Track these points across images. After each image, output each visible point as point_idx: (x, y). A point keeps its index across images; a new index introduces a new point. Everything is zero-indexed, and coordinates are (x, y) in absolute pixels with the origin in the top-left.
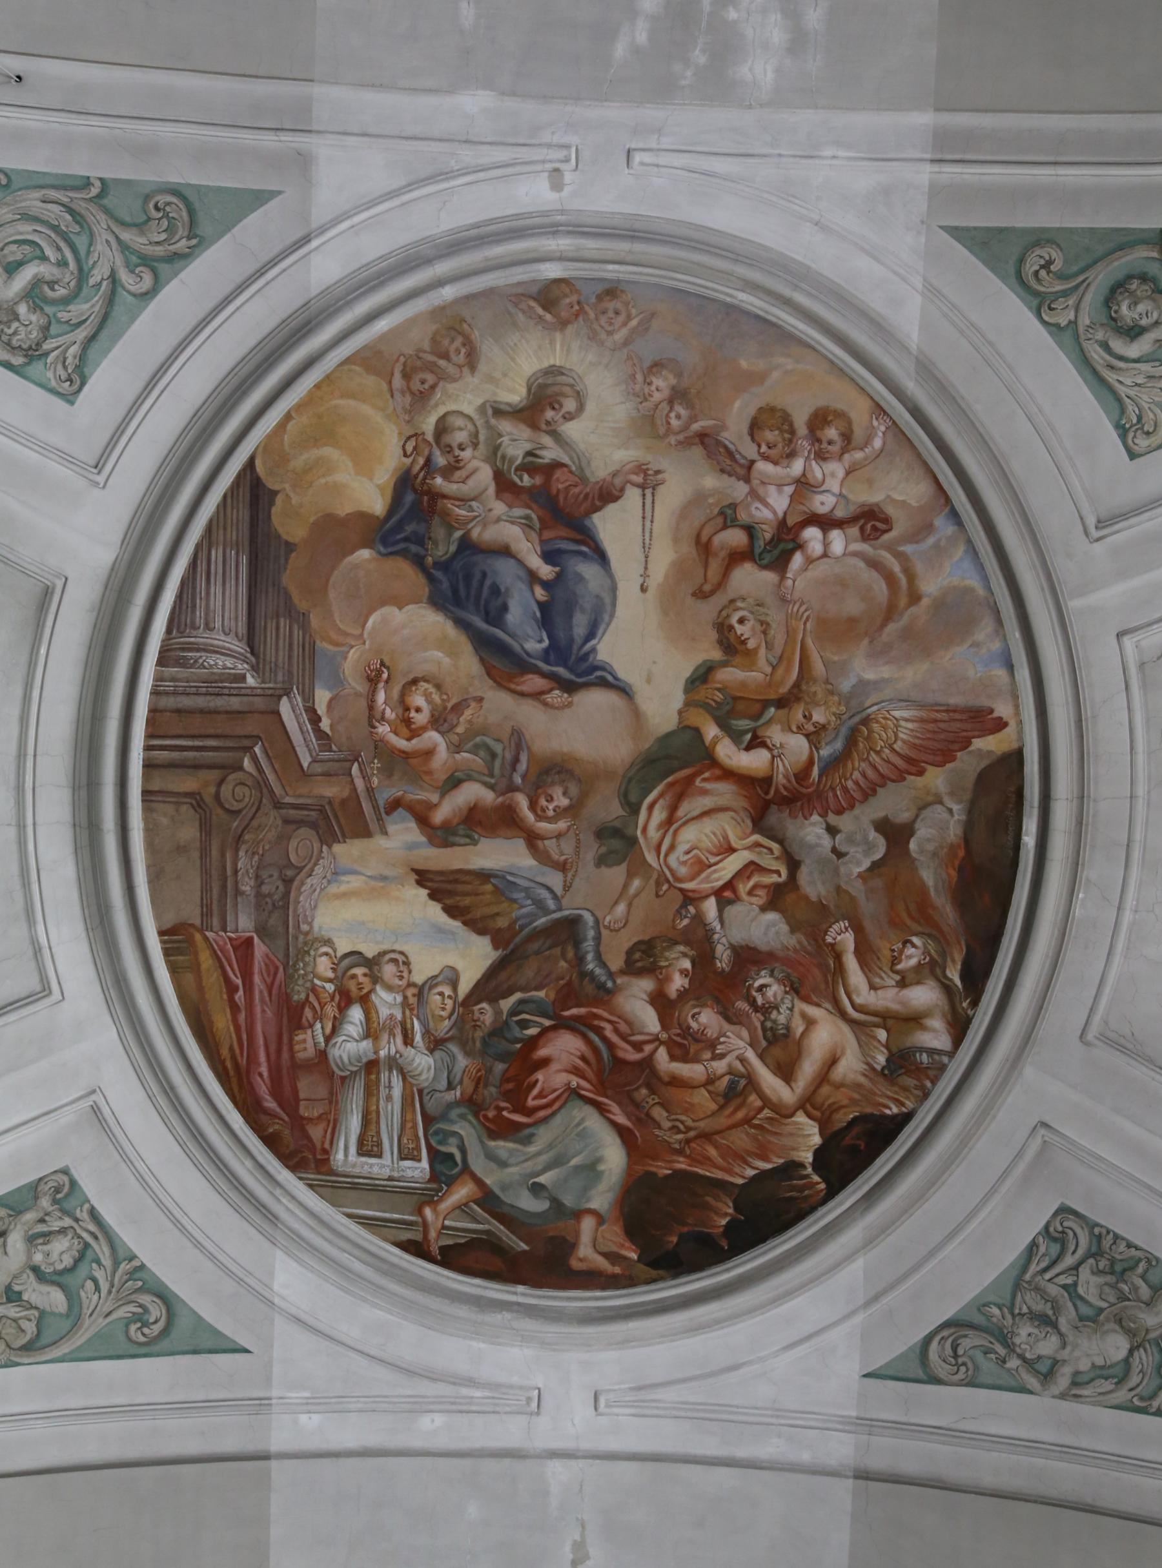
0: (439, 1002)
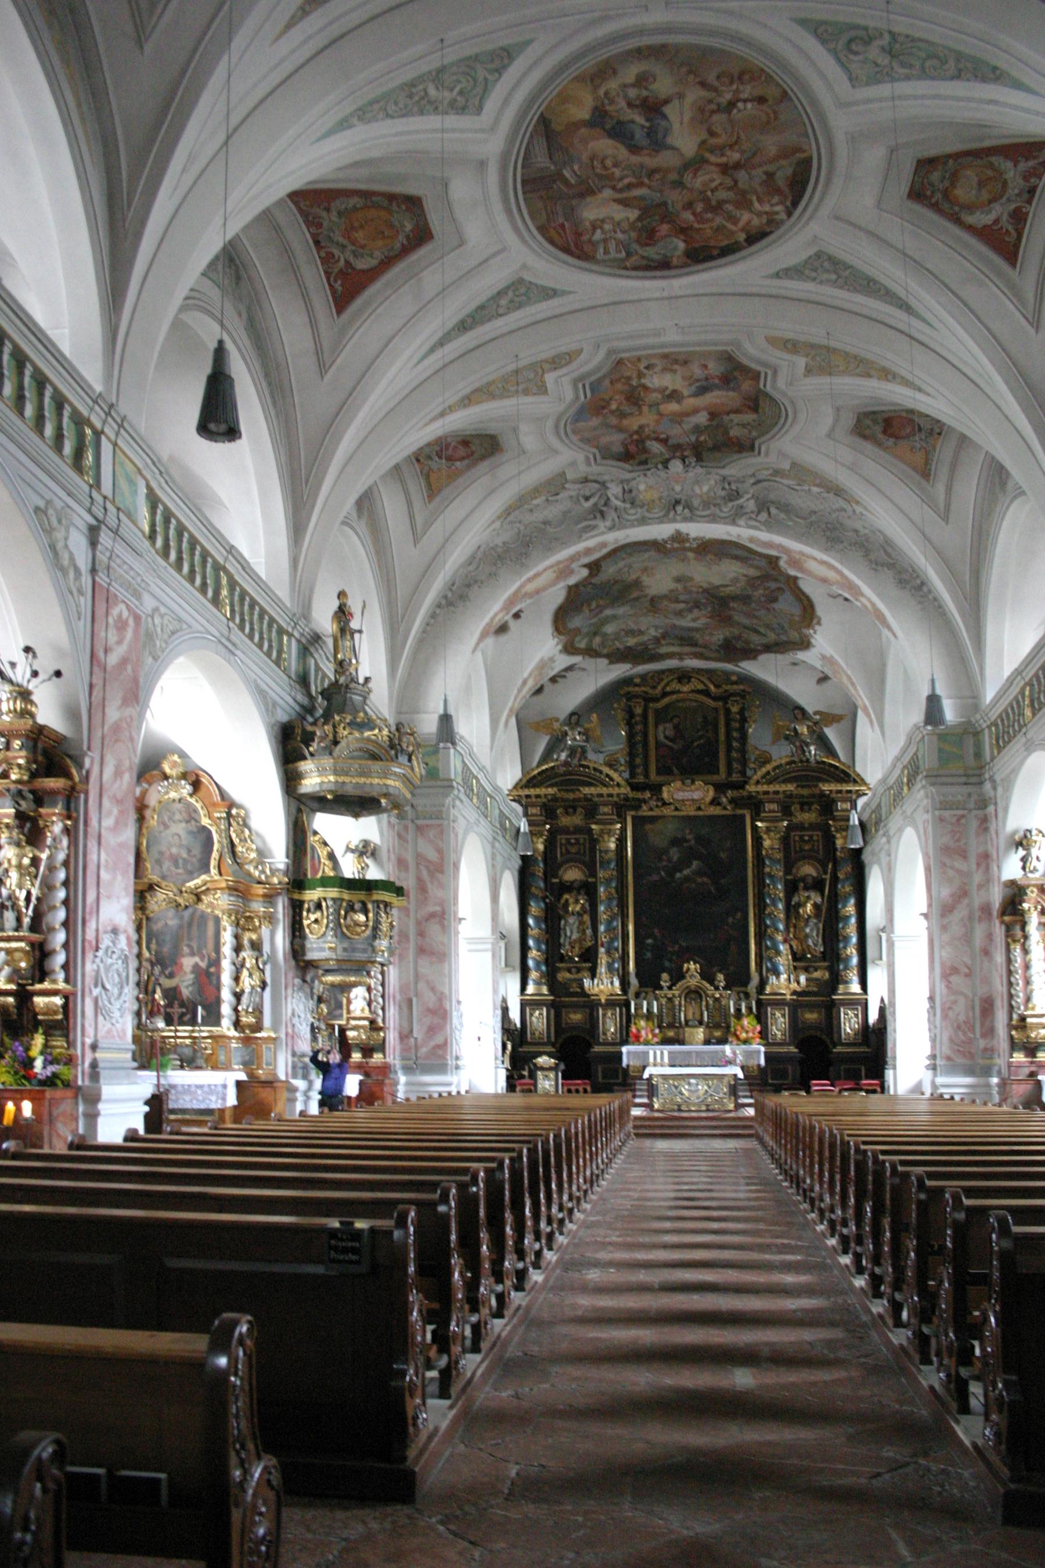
0: (625, 225)
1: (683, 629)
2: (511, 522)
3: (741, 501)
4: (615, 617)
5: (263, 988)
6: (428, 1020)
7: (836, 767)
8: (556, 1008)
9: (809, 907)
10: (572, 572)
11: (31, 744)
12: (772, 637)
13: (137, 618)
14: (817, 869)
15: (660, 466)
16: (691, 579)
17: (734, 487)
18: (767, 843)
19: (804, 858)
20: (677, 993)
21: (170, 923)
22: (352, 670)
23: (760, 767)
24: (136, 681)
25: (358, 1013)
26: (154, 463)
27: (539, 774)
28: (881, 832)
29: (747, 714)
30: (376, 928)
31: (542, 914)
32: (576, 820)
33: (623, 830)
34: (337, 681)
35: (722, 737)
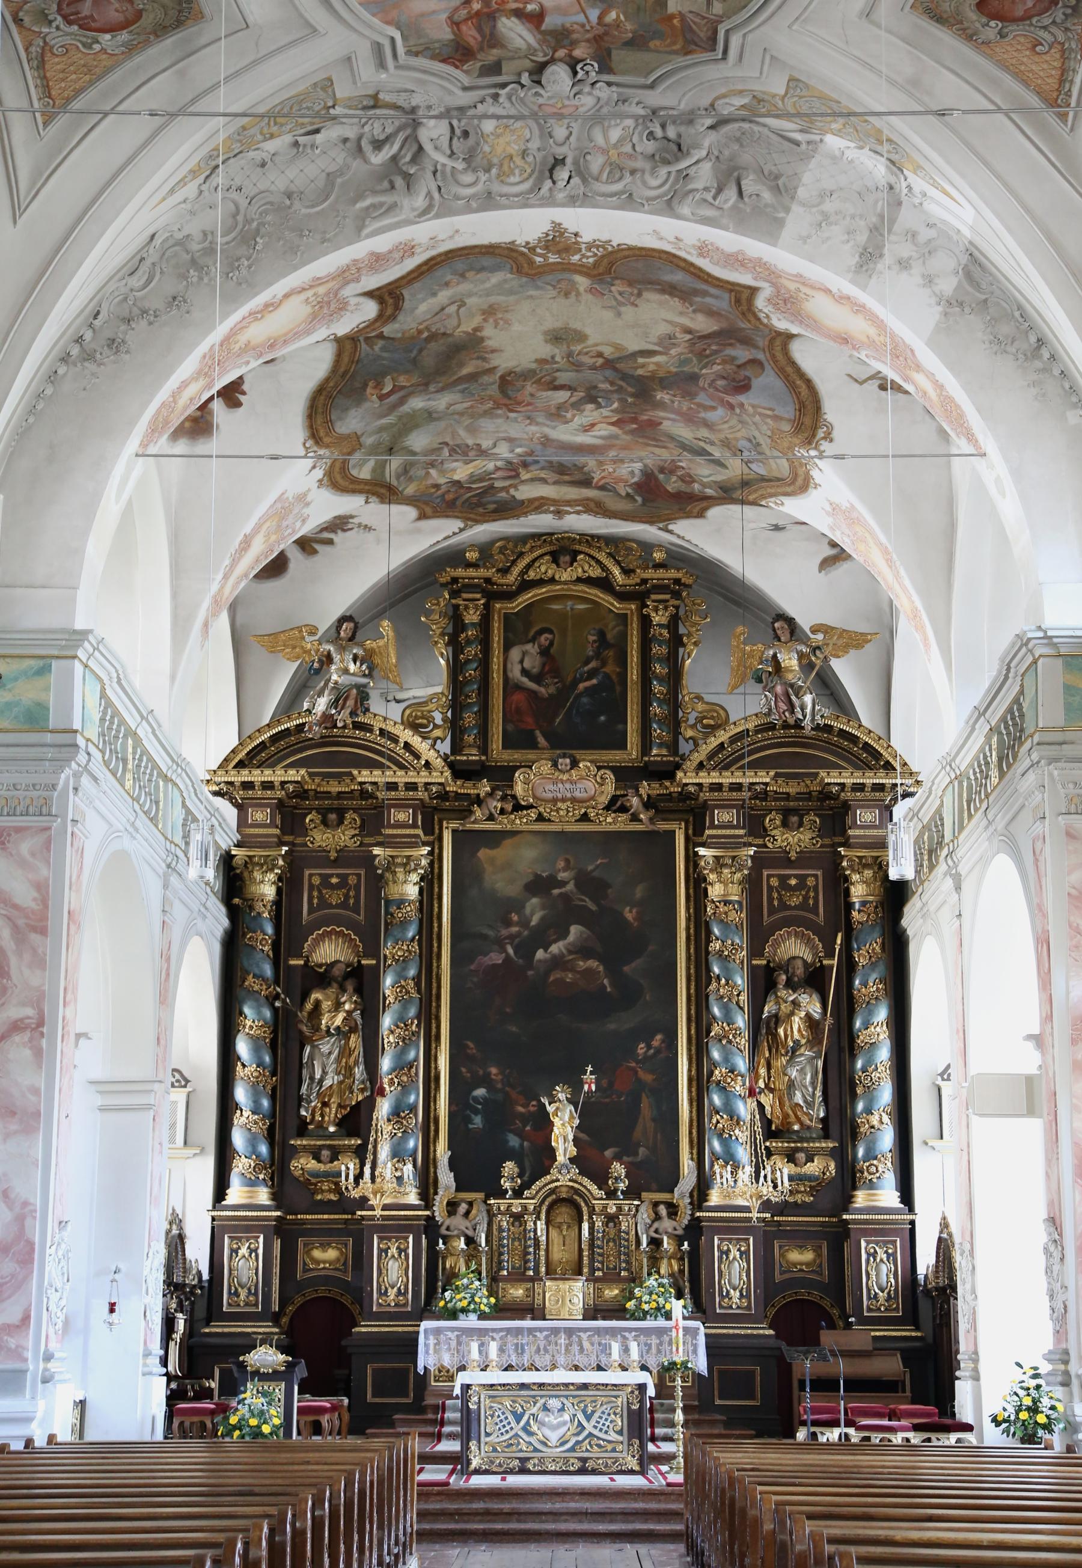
3: (683, 165)
4: (430, 416)
7: (854, 739)
9: (797, 1022)
10: (343, 306)
12: (735, 469)
14: (814, 948)
15: (525, 79)
16: (581, 337)
17: (671, 133)
18: (715, 891)
19: (786, 922)
23: (706, 736)
27: (275, 739)
28: (942, 868)
29: (682, 630)
32: (344, 837)
33: (436, 858)
35: (634, 674)
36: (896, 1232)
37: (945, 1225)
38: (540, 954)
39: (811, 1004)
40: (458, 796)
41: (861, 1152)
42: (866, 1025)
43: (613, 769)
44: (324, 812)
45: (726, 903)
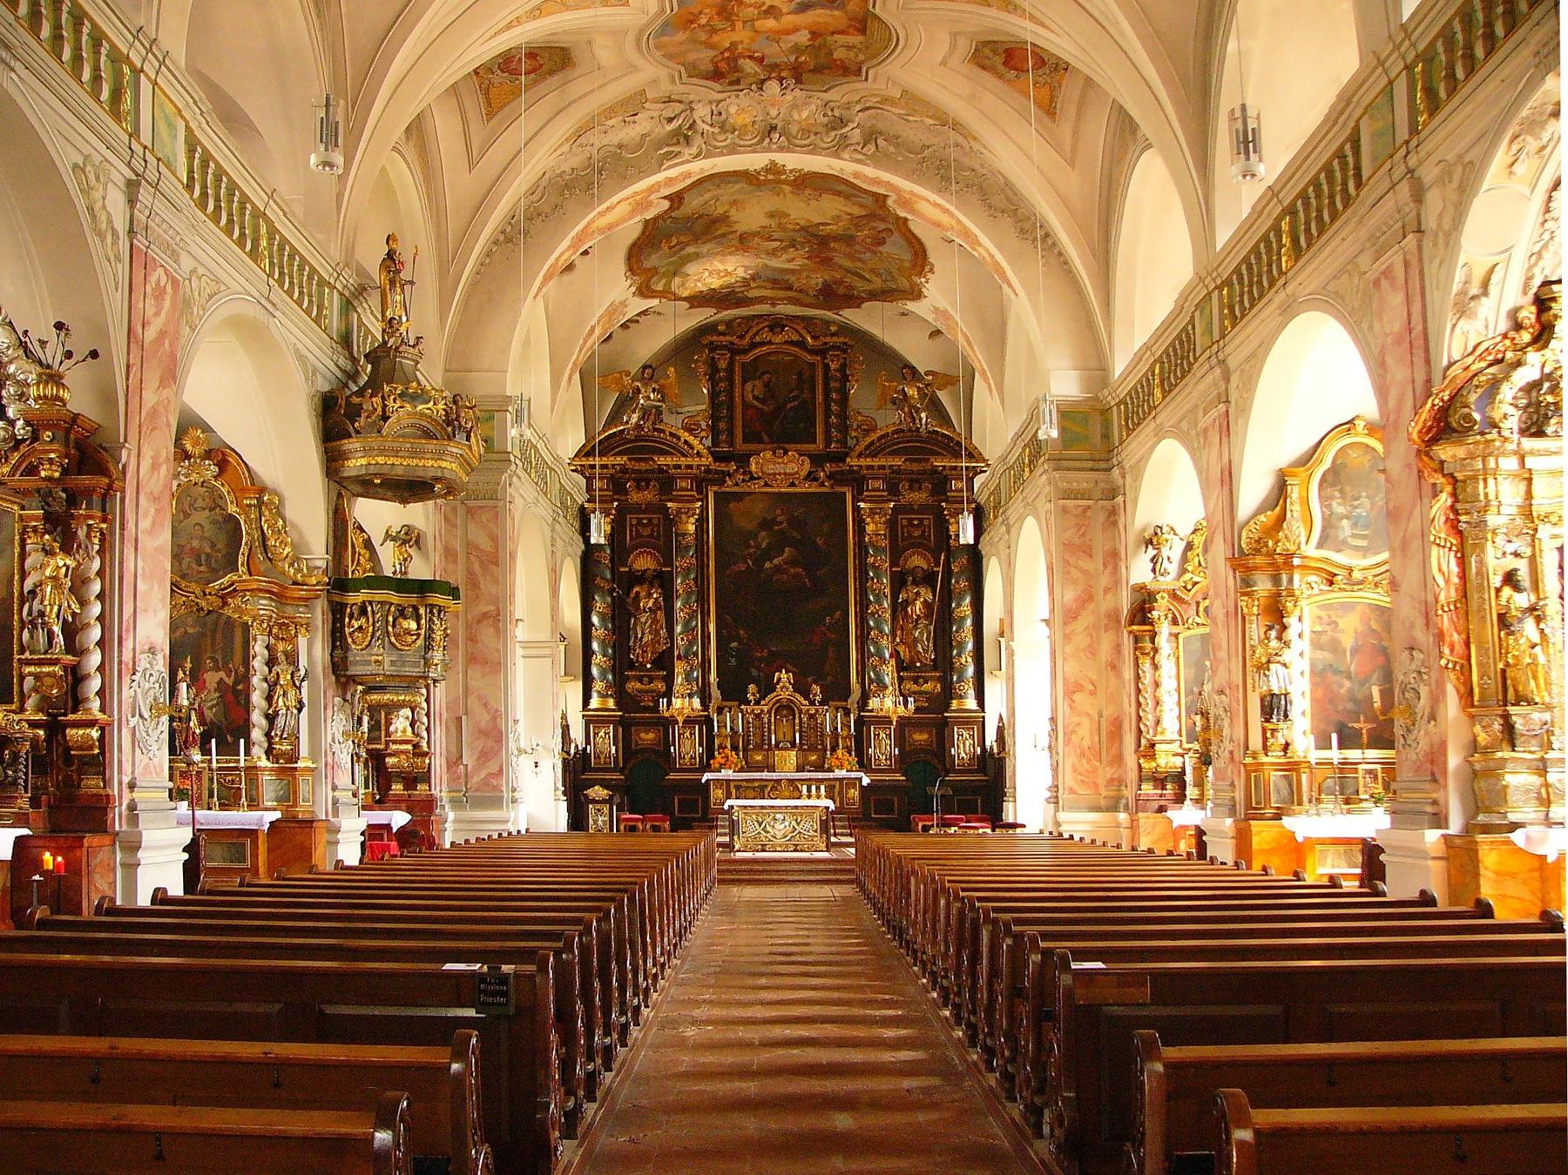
1: (775, 269)
2: (581, 146)
5: (300, 710)
6: (479, 744)
7: (951, 439)
8: (626, 726)
9: (918, 604)
10: (650, 204)
11: (61, 434)
13: (175, 284)
18: (870, 528)
19: (912, 546)
20: (766, 709)
21: (190, 631)
22: (402, 330)
23: (864, 436)
24: (173, 357)
25: (398, 736)
26: (195, 102)
30: (429, 638)
31: (608, 611)
33: (705, 509)
34: (385, 343)
35: (820, 398)
36: (974, 723)
37: (1001, 719)
38: (767, 565)
39: (926, 594)
40: (717, 472)
41: (955, 678)
42: (959, 605)
43: (809, 456)
44: (637, 481)
45: (877, 535)
